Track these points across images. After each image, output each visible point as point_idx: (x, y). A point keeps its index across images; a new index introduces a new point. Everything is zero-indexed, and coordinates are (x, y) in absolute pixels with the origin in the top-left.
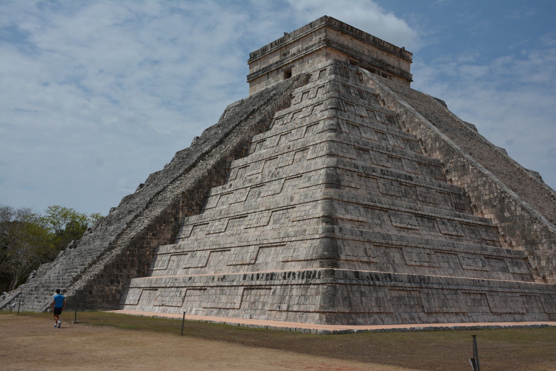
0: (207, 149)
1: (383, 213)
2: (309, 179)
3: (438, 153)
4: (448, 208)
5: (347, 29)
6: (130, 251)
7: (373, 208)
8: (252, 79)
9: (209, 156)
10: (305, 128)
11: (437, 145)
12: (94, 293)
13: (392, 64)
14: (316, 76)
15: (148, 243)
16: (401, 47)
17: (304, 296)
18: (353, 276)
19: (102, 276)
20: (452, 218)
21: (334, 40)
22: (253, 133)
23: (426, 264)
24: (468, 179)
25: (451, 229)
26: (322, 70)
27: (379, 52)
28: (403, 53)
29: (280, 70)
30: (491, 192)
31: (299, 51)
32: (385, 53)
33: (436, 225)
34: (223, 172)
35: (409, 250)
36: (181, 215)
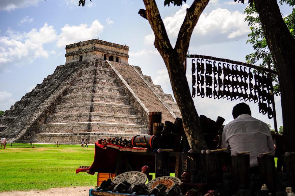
0: (52, 90)
4: (127, 113)
5: (103, 43)
7: (102, 116)
8: (67, 55)
10: (86, 88)
15: (38, 124)
20: (126, 117)
21: (98, 48)
24: (135, 104)
26: (93, 62)
28: (125, 47)
30: (140, 108)
31: (85, 49)
32: (118, 49)
33: (121, 119)
35: (110, 127)
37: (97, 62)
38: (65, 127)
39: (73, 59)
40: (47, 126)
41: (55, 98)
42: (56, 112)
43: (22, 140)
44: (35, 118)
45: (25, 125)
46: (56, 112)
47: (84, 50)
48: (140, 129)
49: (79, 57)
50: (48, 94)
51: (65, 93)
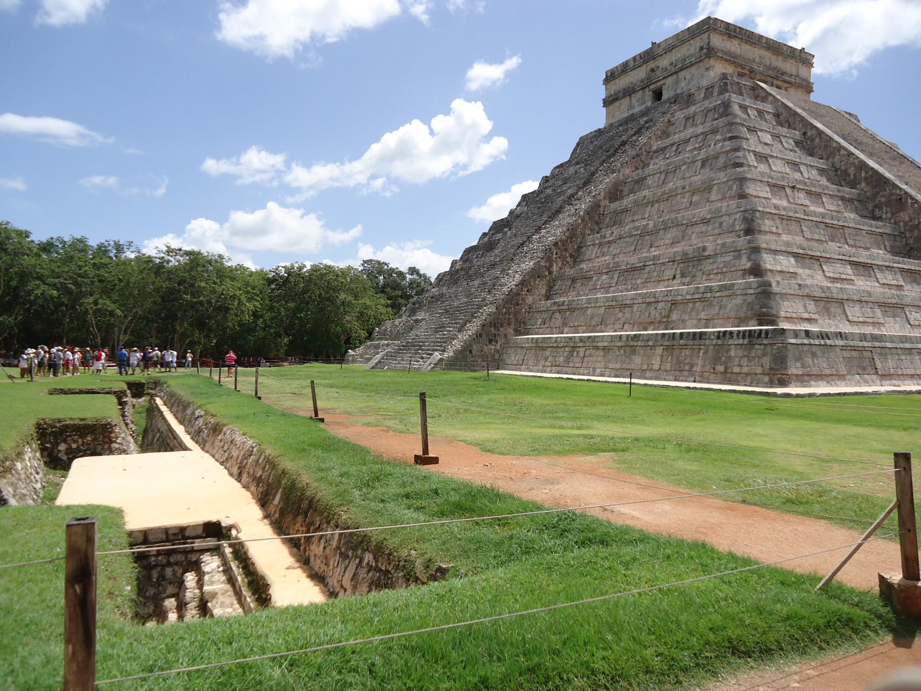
0: (570, 192)
1: (814, 261)
2: (721, 223)
5: (735, 32)
8: (608, 102)
10: (699, 164)
11: (863, 174)
12: (474, 353)
15: (524, 300)
16: (799, 48)
17: (748, 356)
19: (480, 335)
20: (891, 265)
24: (904, 216)
27: (773, 57)
28: (803, 55)
29: (647, 89)
31: (671, 64)
32: (780, 58)
33: (872, 273)
34: (597, 218)
37: (726, 84)
38: (631, 306)
39: (631, 107)
40: (555, 308)
41: (581, 213)
42: (587, 257)
43: (463, 361)
44: (511, 281)
45: (480, 307)
46: (587, 257)
47: (669, 68)
50: (556, 206)
51: (615, 194)
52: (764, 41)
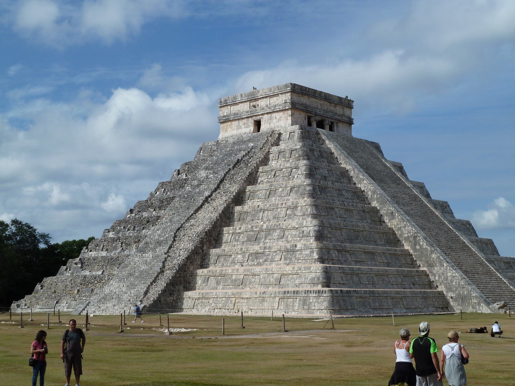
0: (207, 194)
1: (347, 253)
2: (303, 232)
3: (375, 202)
6: (179, 274)
9: (211, 200)
10: (289, 188)
12: (162, 302)
13: (338, 112)
14: (285, 136)
15: (188, 268)
16: (344, 97)
17: (318, 302)
18: (339, 292)
19: (165, 291)
22: (245, 184)
23: (371, 283)
24: (395, 222)
25: (384, 259)
29: (250, 119)
31: (267, 106)
34: (228, 215)
35: (362, 275)
36: (205, 247)
48: (417, 279)
49: (251, 122)
52: (323, 95)
